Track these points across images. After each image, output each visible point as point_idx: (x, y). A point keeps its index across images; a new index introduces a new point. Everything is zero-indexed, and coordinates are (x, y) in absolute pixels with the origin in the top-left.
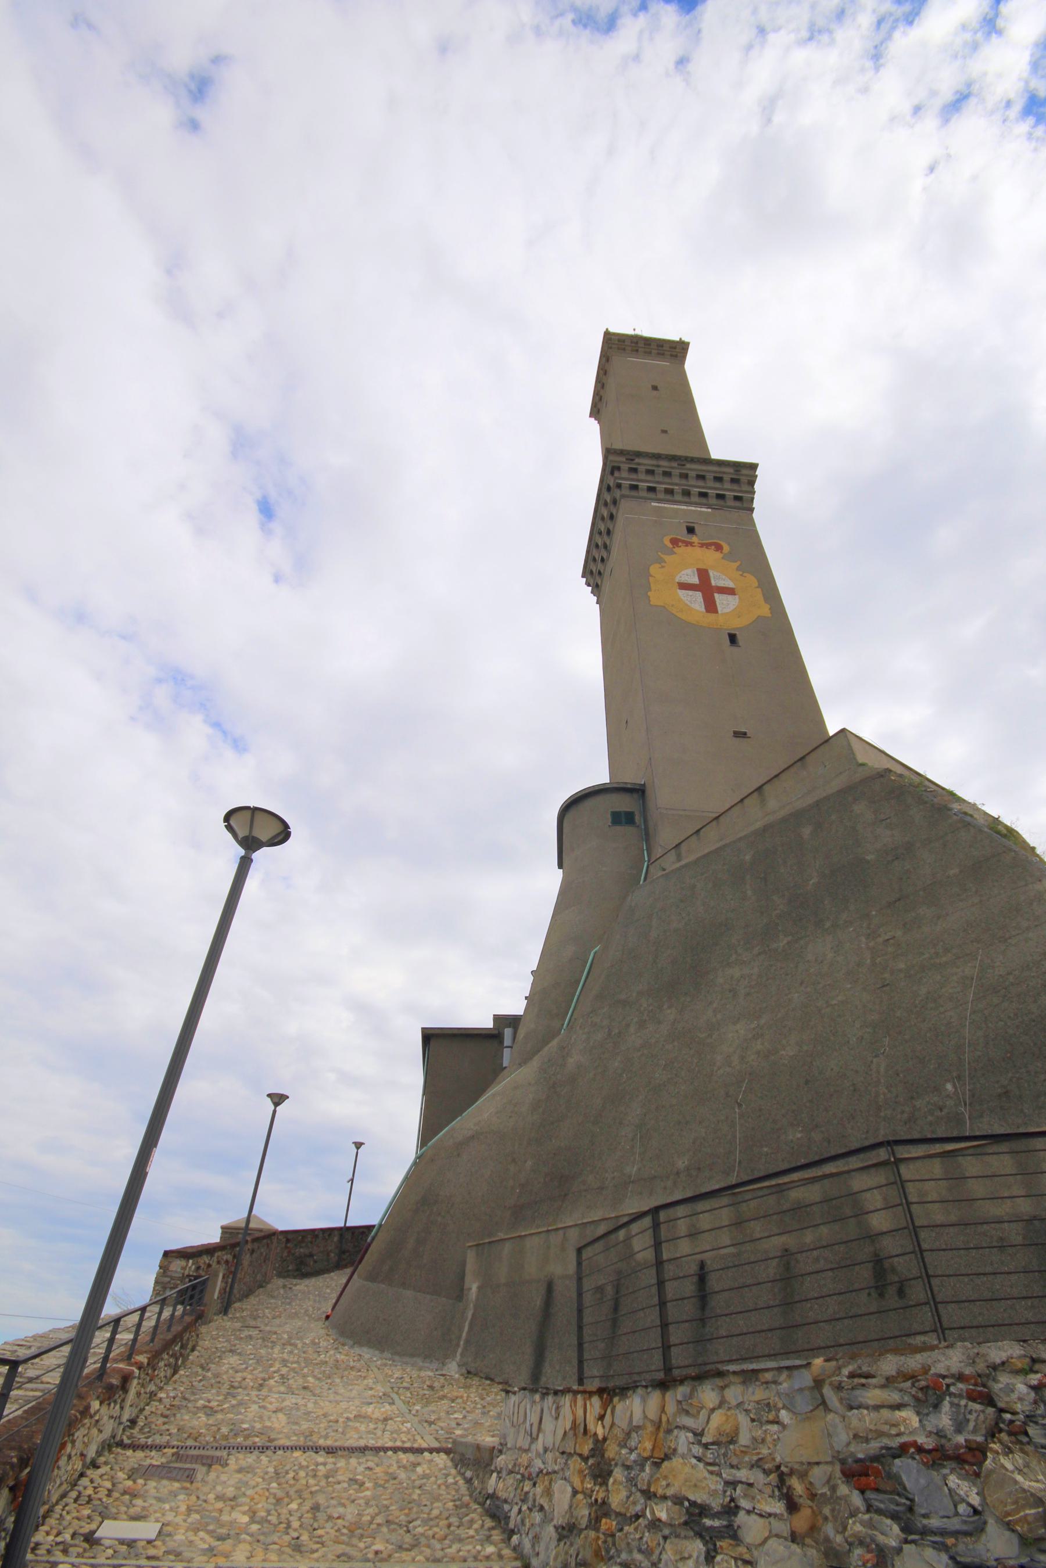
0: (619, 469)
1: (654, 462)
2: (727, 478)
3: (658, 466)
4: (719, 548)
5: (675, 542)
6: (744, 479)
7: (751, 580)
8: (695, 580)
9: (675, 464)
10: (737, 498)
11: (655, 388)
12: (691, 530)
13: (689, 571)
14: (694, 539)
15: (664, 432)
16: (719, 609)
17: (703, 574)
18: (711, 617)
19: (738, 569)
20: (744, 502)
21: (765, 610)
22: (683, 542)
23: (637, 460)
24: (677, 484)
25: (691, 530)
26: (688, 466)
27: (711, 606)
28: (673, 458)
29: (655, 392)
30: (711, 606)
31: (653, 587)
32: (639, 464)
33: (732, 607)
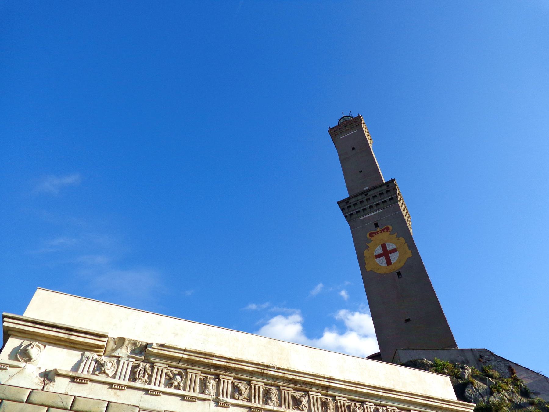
0: (344, 209)
1: (356, 199)
2: (384, 192)
3: (357, 200)
4: (388, 229)
5: (371, 235)
6: (391, 189)
7: (402, 240)
8: (381, 251)
9: (364, 196)
10: (390, 199)
11: (353, 149)
12: (376, 225)
13: (378, 248)
14: (378, 229)
15: (361, 172)
16: (392, 261)
17: (384, 246)
18: (390, 266)
19: (396, 237)
20: (394, 200)
21: (409, 254)
22: (374, 233)
23: (350, 201)
24: (366, 205)
25: (376, 225)
26: (369, 193)
27: (389, 262)
28: (362, 194)
29: (354, 151)
30: (389, 262)
31: (366, 262)
32: (350, 203)
33: (397, 258)
